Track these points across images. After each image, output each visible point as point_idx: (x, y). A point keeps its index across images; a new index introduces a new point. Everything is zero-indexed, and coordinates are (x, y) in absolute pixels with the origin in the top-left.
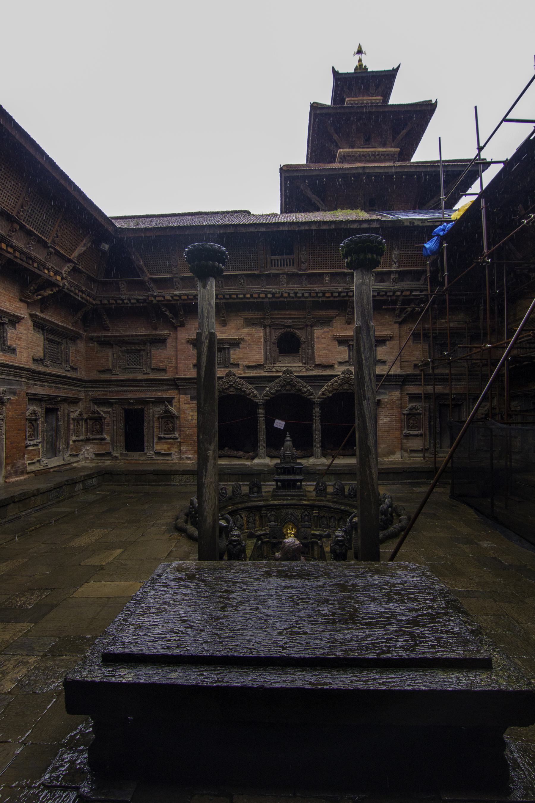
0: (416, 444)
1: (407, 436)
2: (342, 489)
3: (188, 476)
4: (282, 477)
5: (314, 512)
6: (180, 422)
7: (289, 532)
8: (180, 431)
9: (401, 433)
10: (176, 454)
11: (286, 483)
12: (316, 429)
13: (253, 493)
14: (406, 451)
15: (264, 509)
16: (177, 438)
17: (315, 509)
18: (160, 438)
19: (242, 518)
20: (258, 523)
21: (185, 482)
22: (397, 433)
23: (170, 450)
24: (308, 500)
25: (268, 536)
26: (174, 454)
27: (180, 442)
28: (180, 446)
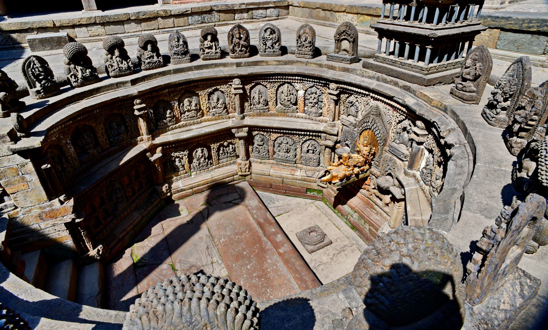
3: (352, 15)
15: (333, 86)
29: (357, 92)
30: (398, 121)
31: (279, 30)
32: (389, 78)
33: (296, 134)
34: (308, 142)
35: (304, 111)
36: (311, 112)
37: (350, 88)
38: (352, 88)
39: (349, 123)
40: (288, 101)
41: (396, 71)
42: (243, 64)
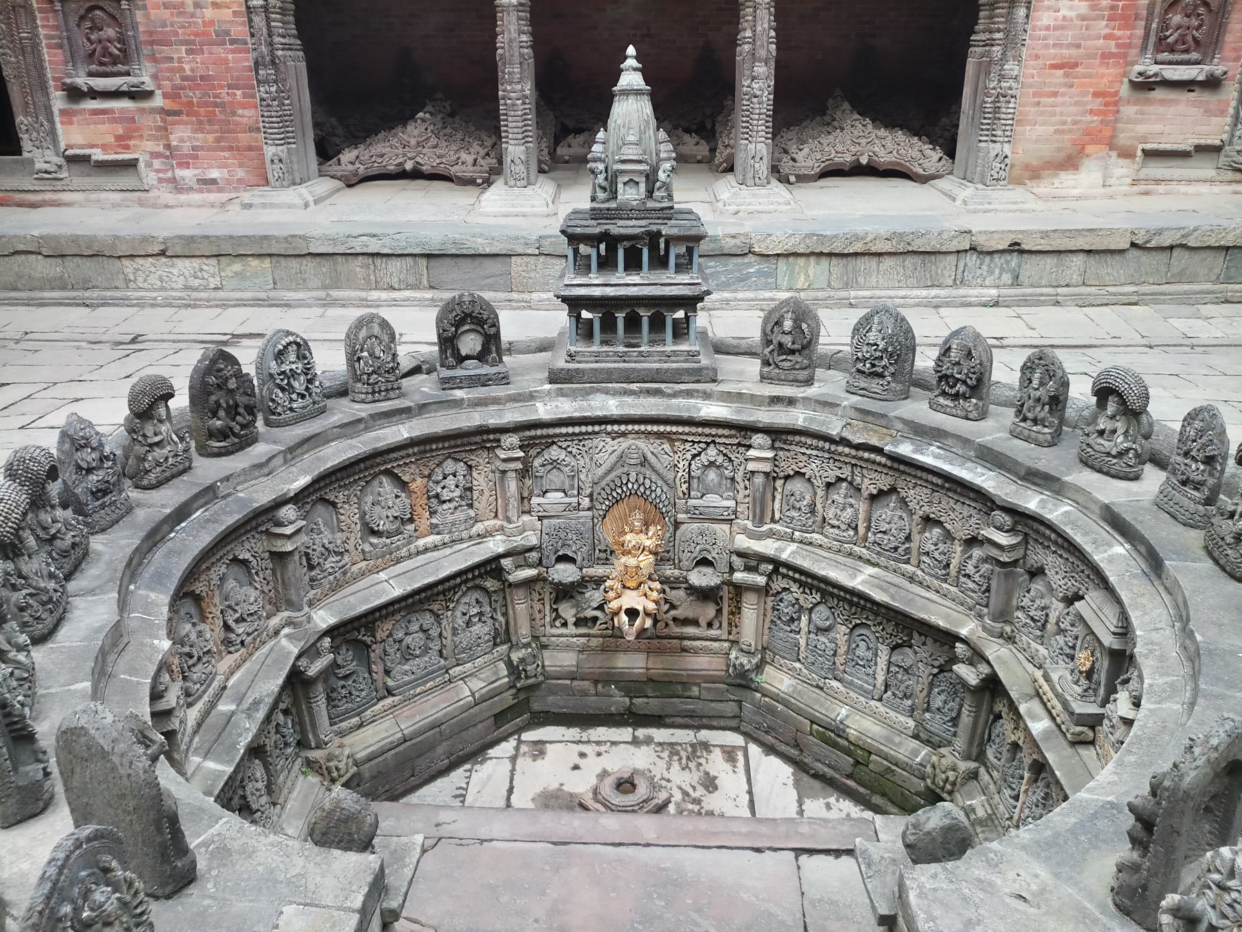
0: (1179, 121)
1: (1145, 85)
2: (901, 348)
3: (196, 263)
4: (597, 285)
5: (752, 453)
6: (147, 16)
7: (631, 539)
8: (154, 59)
9: (1124, 75)
10: (157, 163)
11: (620, 316)
12: (753, 54)
13: (461, 359)
14: (1127, 154)
15: (512, 440)
16: (149, 95)
17: (758, 439)
18: (75, 94)
19: (403, 485)
20: (483, 503)
21: (186, 288)
22: (1107, 76)
23: (127, 147)
24: (728, 397)
25: (534, 555)
26: (149, 165)
27: (162, 111)
28: (165, 130)
29: (567, 435)
30: (690, 457)
31: (305, 342)
32: (634, 386)
33: (438, 594)
34: (464, 600)
35: (434, 529)
36: (453, 524)
37: (551, 431)
38: (557, 431)
39: (562, 507)
40: (396, 518)
41: (645, 370)
42: (278, 461)
